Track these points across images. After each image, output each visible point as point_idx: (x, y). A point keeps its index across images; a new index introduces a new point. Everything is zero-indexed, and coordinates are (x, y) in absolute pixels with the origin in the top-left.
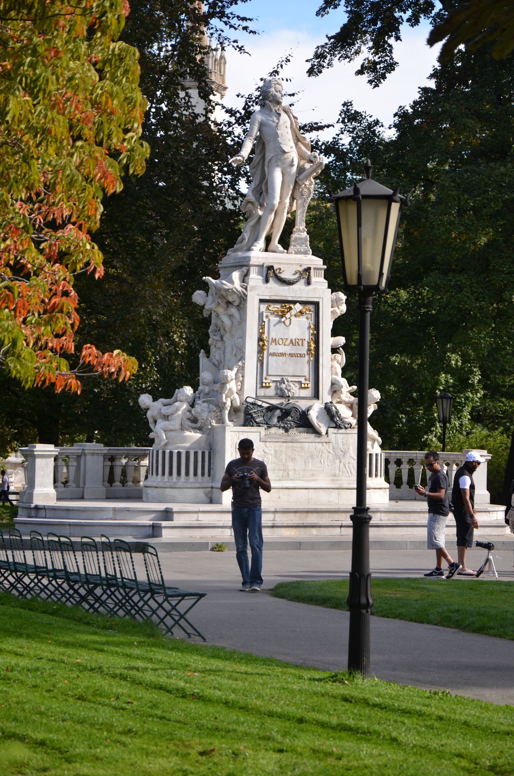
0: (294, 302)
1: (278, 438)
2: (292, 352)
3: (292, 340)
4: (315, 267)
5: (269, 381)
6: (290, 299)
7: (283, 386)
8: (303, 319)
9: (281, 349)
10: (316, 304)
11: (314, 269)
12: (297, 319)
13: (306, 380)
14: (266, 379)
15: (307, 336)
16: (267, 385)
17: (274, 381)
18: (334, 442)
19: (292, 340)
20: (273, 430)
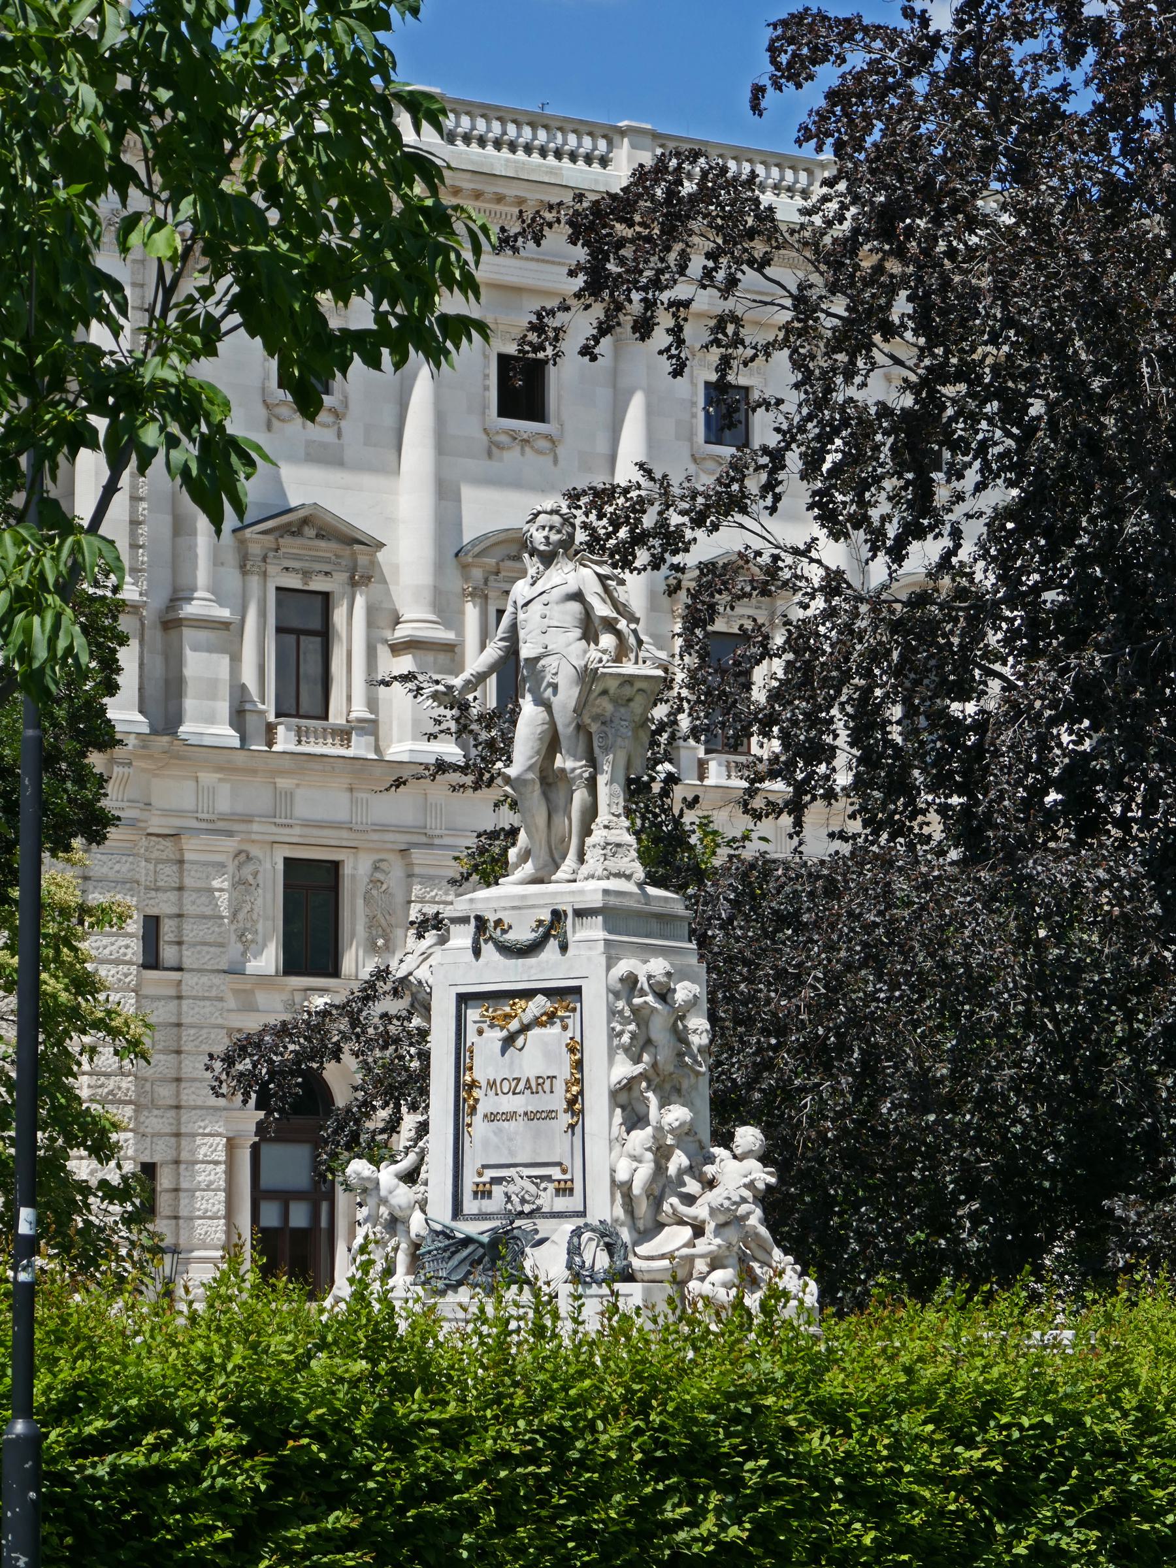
0: (528, 994)
7: (511, 1188)
8: (556, 1029)
9: (508, 1103)
10: (577, 991)
12: (543, 1031)
13: (564, 1172)
14: (480, 1175)
15: (564, 1071)
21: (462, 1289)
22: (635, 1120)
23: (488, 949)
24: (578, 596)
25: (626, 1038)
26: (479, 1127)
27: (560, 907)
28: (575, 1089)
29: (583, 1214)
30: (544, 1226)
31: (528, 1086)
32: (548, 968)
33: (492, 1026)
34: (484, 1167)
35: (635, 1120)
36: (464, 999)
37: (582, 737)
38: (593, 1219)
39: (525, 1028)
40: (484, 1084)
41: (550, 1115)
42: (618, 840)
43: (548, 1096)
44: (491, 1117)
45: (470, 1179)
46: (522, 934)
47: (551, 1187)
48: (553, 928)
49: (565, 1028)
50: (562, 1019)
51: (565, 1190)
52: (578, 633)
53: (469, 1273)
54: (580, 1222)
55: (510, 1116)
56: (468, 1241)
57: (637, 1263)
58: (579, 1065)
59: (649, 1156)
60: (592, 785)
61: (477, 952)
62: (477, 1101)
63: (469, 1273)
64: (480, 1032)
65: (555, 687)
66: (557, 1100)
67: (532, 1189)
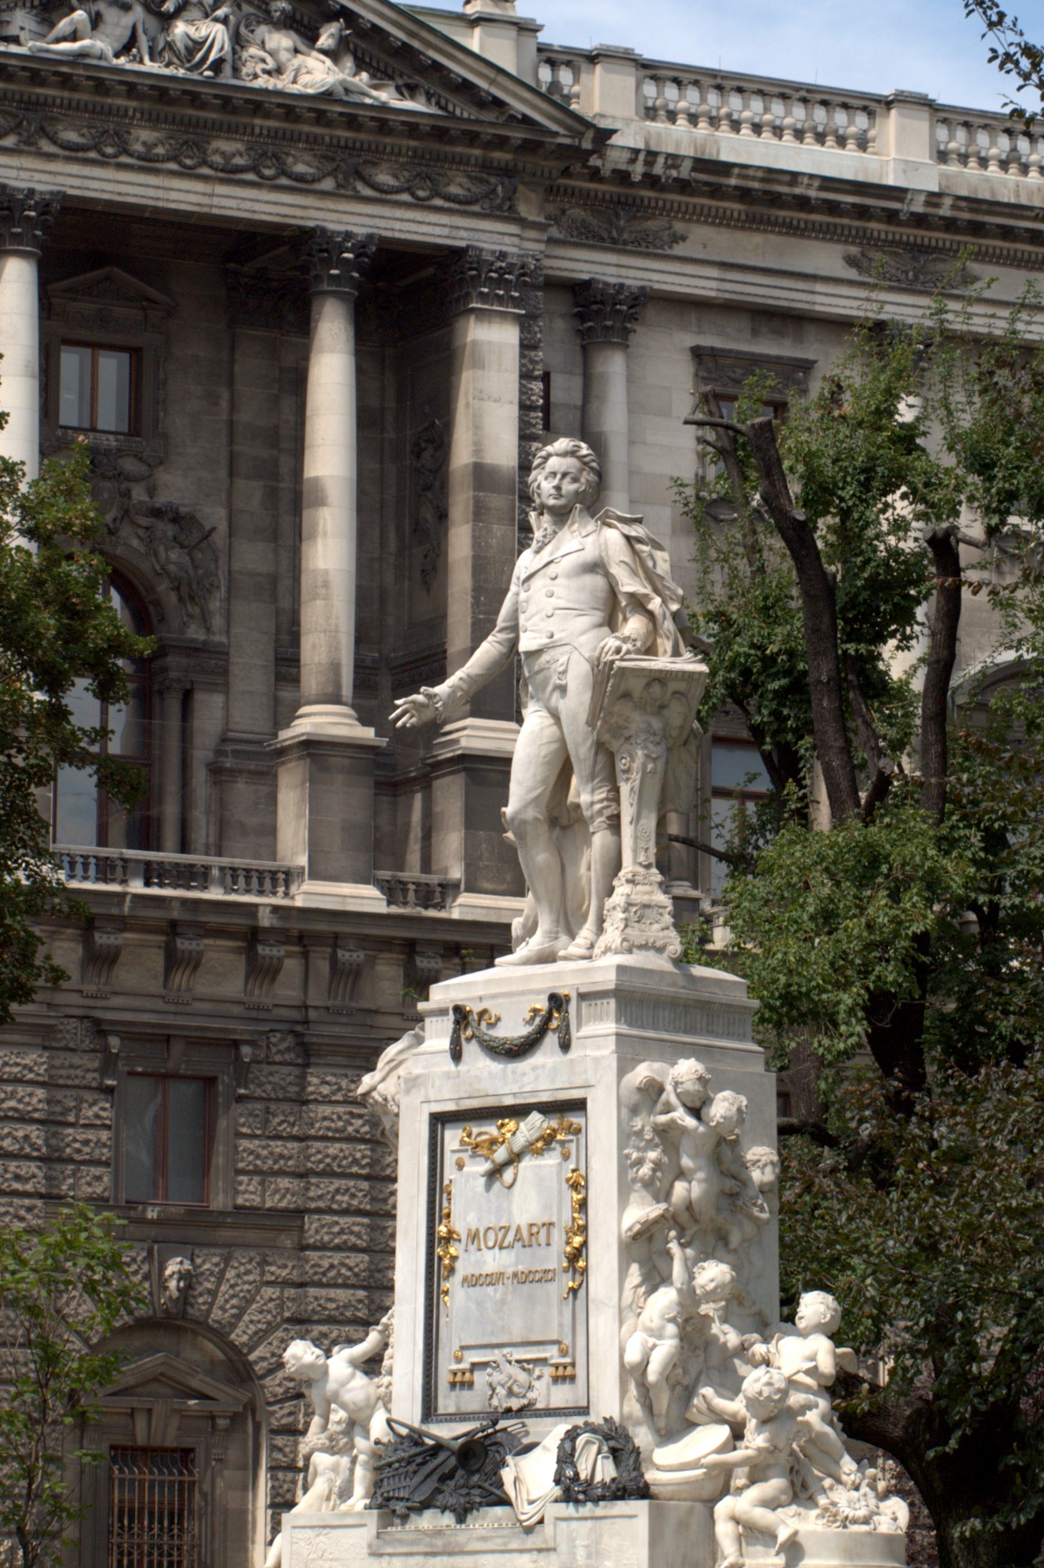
0: (519, 1112)
1: (413, 1543)
2: (521, 1268)
3: (518, 1230)
4: (583, 990)
5: (462, 1366)
6: (509, 1101)
8: (551, 1160)
9: (493, 1261)
10: (579, 1106)
11: (583, 997)
13: (564, 1353)
14: (459, 1360)
15: (566, 1216)
16: (459, 1378)
17: (475, 1366)
18: (563, 1548)
19: (518, 1230)
20: (428, 1520)
21: (428, 1514)
22: (655, 1278)
23: (471, 1050)
24: (597, 567)
25: (645, 1170)
26: (457, 1297)
27: (562, 992)
28: (577, 1240)
29: (584, 1411)
30: (535, 1426)
31: (518, 1237)
32: (541, 1075)
33: (474, 1155)
34: (463, 1348)
35: (655, 1278)
36: (439, 1121)
37: (601, 758)
38: (595, 1418)
39: (515, 1158)
40: (464, 1237)
41: (546, 1276)
42: (645, 899)
43: (542, 1251)
44: (472, 1281)
45: (446, 1366)
46: (513, 1028)
47: (548, 1372)
48: (553, 1020)
49: (566, 1157)
50: (562, 1143)
51: (564, 1377)
52: (598, 616)
53: (438, 1491)
54: (580, 1421)
55: (494, 1279)
56: (439, 1447)
57: (651, 1476)
58: (583, 1206)
59: (671, 1329)
60: (615, 824)
61: (457, 1055)
62: (454, 1258)
63: (438, 1491)
64: (460, 1166)
65: (563, 689)
66: (553, 1257)
67: (522, 1377)
